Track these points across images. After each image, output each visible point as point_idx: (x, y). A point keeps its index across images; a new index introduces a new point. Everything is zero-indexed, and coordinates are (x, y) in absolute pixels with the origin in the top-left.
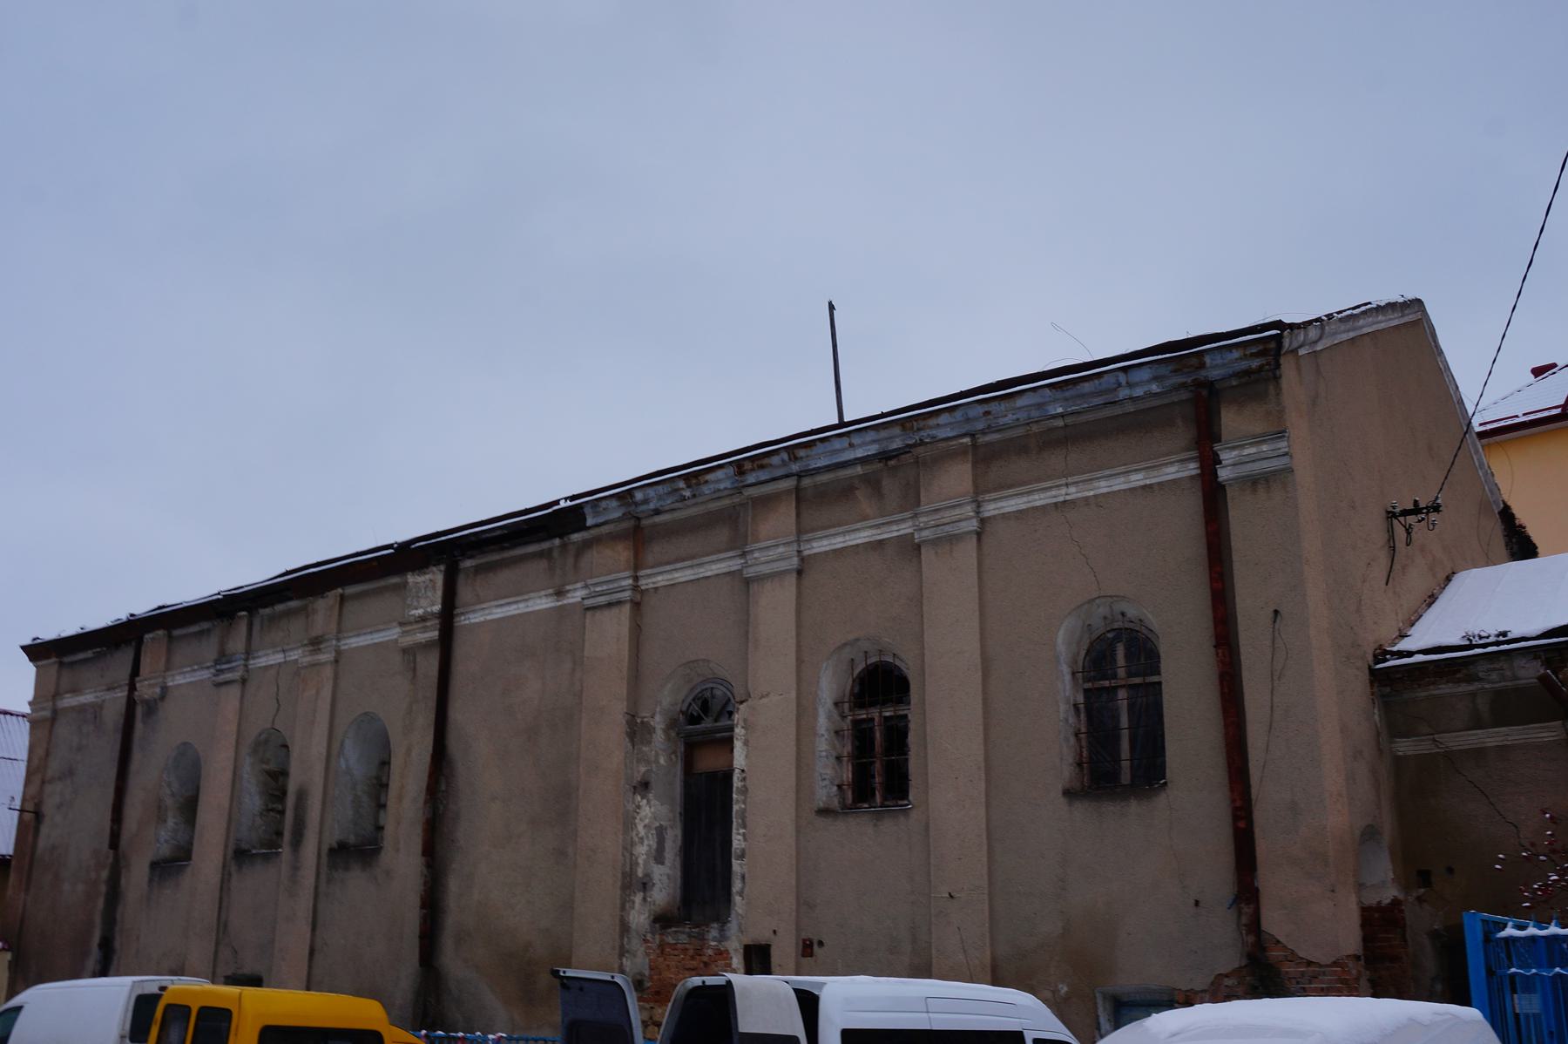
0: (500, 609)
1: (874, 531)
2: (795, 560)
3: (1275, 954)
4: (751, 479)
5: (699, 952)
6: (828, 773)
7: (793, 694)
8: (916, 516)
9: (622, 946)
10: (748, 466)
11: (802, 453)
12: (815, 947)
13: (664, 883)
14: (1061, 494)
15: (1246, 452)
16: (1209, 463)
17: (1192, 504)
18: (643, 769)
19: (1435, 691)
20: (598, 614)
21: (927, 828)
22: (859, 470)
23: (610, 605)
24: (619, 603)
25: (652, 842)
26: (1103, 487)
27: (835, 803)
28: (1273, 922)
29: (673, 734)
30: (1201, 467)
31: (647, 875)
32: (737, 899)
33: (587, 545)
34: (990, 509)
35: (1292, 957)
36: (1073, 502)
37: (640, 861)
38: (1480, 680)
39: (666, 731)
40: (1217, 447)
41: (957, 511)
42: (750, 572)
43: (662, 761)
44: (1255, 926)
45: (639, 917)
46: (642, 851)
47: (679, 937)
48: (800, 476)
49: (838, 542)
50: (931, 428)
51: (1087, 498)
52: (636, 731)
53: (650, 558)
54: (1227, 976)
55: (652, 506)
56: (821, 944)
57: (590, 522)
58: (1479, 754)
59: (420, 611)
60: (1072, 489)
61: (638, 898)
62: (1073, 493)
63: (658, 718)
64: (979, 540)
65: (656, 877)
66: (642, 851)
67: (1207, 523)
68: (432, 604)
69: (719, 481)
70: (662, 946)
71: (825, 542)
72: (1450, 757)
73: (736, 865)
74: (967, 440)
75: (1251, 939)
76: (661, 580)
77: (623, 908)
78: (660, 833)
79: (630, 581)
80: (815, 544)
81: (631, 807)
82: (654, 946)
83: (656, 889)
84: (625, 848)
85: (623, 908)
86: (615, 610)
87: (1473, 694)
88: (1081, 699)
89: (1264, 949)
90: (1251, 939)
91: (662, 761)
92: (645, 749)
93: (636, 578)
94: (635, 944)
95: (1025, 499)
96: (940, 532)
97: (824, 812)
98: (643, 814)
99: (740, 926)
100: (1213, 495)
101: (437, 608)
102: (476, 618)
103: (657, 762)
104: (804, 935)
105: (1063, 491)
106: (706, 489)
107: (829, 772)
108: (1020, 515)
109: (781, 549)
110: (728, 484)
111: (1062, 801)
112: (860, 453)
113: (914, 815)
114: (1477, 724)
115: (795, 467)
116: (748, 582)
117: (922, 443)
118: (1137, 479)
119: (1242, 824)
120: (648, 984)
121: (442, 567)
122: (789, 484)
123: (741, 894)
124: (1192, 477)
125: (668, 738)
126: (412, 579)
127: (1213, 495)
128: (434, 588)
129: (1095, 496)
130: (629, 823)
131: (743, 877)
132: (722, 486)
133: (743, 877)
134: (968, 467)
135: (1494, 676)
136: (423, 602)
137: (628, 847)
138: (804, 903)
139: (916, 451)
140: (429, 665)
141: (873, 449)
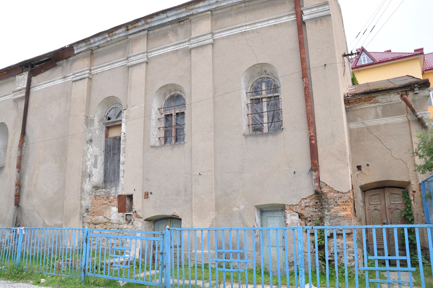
0: (46, 84)
1: (175, 47)
2: (146, 59)
3: (325, 190)
4: (131, 32)
5: (108, 198)
6: (156, 133)
7: (143, 105)
8: (190, 40)
9: (81, 197)
10: (130, 27)
11: (149, 21)
12: (149, 195)
13: (97, 176)
14: (243, 29)
15: (313, 10)
16: (299, 14)
17: (293, 30)
18: (90, 135)
19: (363, 107)
20: (77, 83)
21: (191, 150)
22: (170, 26)
23: (81, 79)
24: (84, 78)
25: (93, 160)
26: (259, 26)
27: (158, 144)
28: (325, 177)
29: (102, 124)
30: (297, 17)
31: (91, 172)
32: (121, 179)
33: (75, 61)
34: (217, 36)
35: (332, 190)
36: (248, 31)
37: (88, 167)
38: (379, 102)
39: (99, 122)
40: (302, 9)
41: (205, 37)
42: (130, 64)
43: (97, 132)
44: (318, 179)
45: (88, 187)
46: (89, 163)
47: (102, 192)
48: (149, 30)
49: (161, 52)
50: (196, 8)
51: (253, 30)
52: (88, 122)
53: (96, 64)
54: (306, 199)
55: (97, 44)
56: (151, 193)
57: (75, 53)
58: (378, 127)
59: (20, 88)
60: (248, 27)
61: (88, 179)
62: (248, 28)
63: (96, 118)
64: (213, 47)
65: (94, 173)
66: (89, 163)
67: (299, 35)
68: (24, 85)
69: (119, 33)
70: (95, 196)
71: (157, 52)
72: (368, 128)
73: (121, 167)
74: (209, 12)
75: (317, 184)
76: (99, 70)
77: (82, 183)
78: (96, 157)
79: (88, 71)
80: (153, 53)
81: (85, 148)
82: (92, 196)
83: (94, 177)
84: (83, 163)
85: (82, 183)
86: (82, 81)
87: (376, 107)
88: (249, 102)
89: (321, 188)
90: (317, 184)
91: (97, 132)
92: (91, 128)
93: (90, 70)
94: (86, 196)
95: (230, 32)
96: (198, 44)
97: (153, 147)
98: (90, 151)
99: (122, 188)
100: (301, 25)
101: (25, 86)
102: (38, 88)
103: (95, 132)
104: (145, 191)
105: (244, 28)
106: (115, 37)
107: (156, 133)
108: (228, 37)
109: (141, 56)
110: (123, 35)
111: (243, 137)
112: (170, 19)
113: (186, 145)
114: (377, 116)
115: (146, 27)
116: (129, 67)
117: (193, 15)
118: (272, 22)
119: (313, 142)
120: (90, 210)
121: (27, 72)
122: (146, 32)
123: (123, 177)
124: (293, 21)
125: (100, 125)
126: (18, 77)
127: (301, 25)
128: (24, 80)
129: (256, 29)
130: (84, 154)
131: (124, 171)
132: (121, 35)
133: (124, 171)
134: (209, 22)
135: (384, 101)
136: (21, 85)
137: (84, 162)
138: (146, 179)
139: (190, 18)
140: (22, 105)
141: (175, 18)
